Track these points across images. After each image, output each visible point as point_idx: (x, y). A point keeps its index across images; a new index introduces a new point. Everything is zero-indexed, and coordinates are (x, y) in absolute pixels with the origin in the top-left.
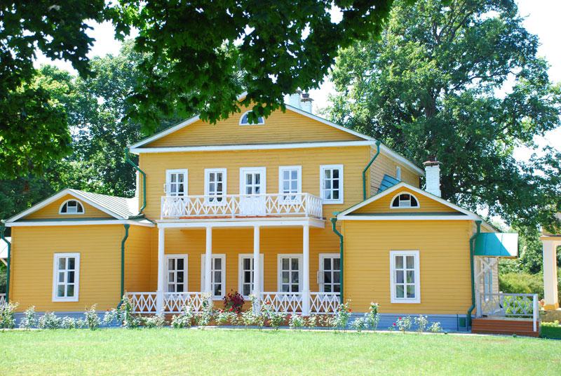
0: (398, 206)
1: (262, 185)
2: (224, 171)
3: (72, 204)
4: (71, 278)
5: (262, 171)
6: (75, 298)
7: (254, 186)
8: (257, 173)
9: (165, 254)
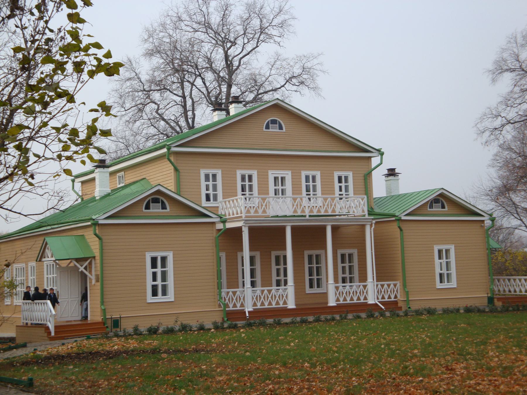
0: (150, 209)
1: (288, 186)
7: (280, 187)
8: (283, 176)
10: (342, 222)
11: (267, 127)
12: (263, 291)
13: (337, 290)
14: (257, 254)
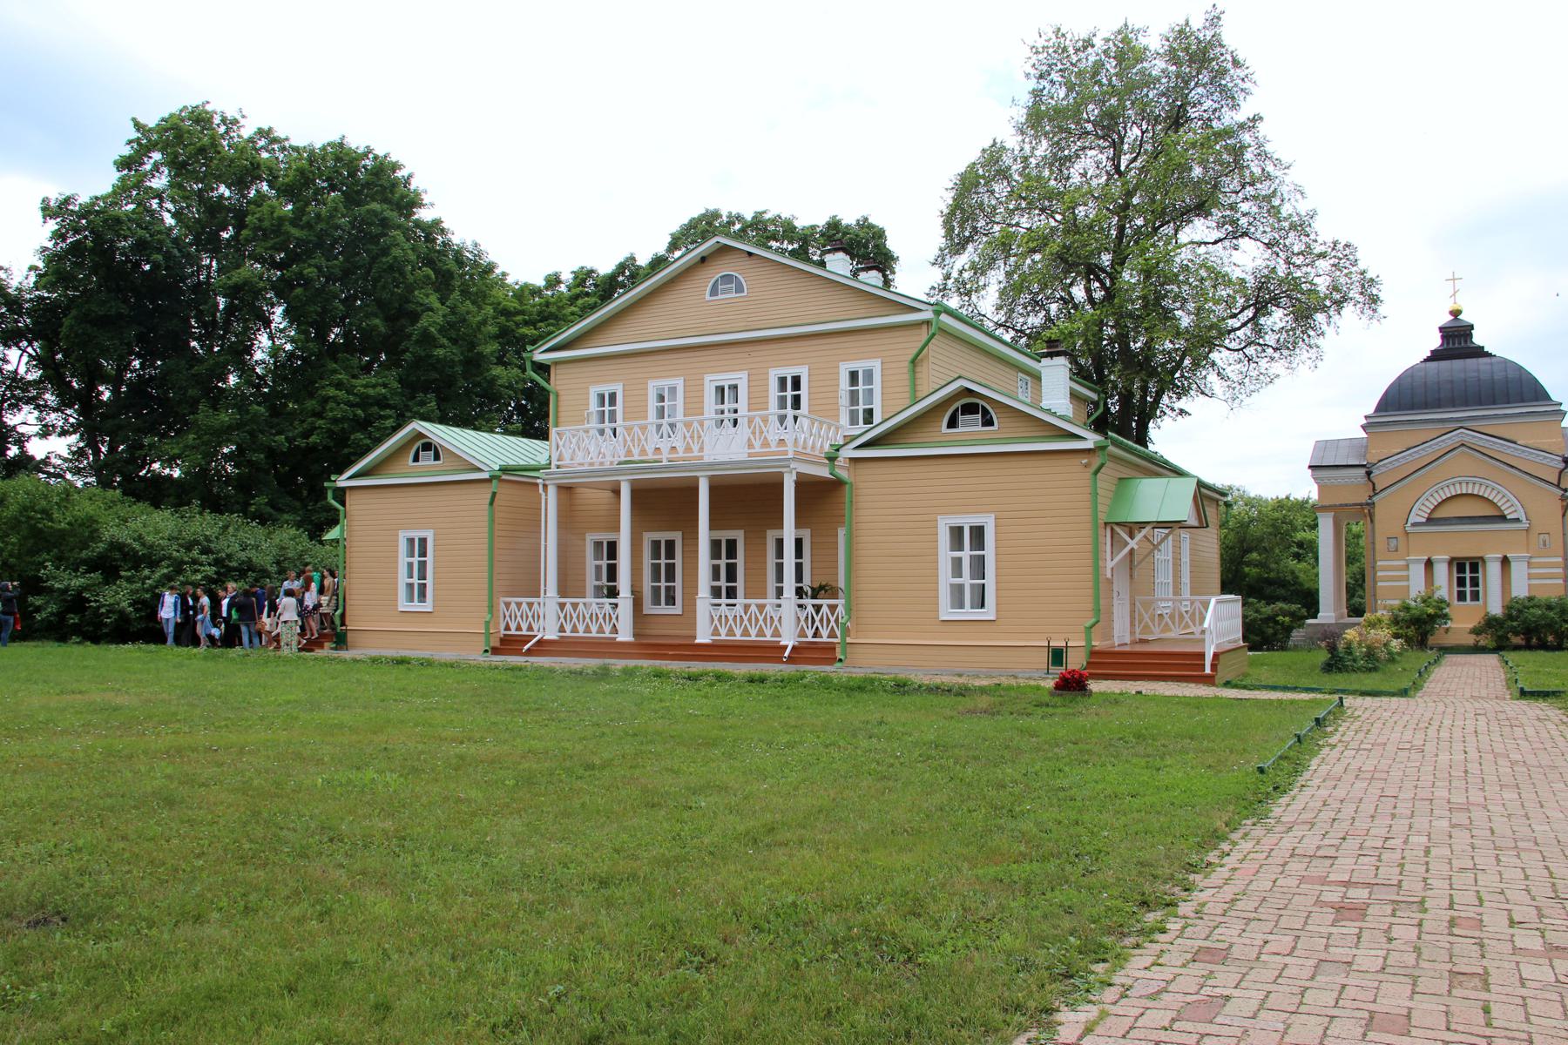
2: (679, 383)
3: (427, 446)
4: (979, 567)
5: (741, 379)
6: (989, 613)
9: (710, 529)
10: (572, 478)
11: (714, 292)
12: (747, 607)
13: (562, 610)
14: (806, 534)
